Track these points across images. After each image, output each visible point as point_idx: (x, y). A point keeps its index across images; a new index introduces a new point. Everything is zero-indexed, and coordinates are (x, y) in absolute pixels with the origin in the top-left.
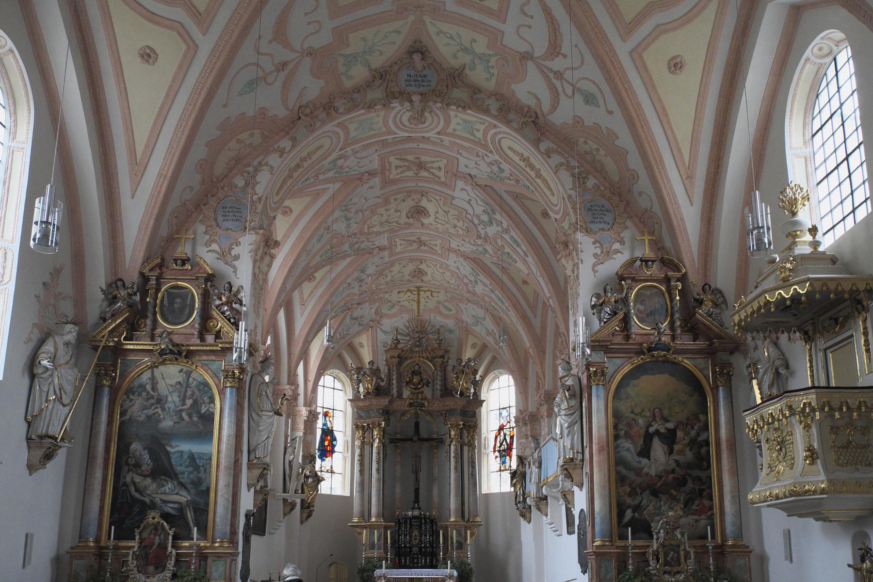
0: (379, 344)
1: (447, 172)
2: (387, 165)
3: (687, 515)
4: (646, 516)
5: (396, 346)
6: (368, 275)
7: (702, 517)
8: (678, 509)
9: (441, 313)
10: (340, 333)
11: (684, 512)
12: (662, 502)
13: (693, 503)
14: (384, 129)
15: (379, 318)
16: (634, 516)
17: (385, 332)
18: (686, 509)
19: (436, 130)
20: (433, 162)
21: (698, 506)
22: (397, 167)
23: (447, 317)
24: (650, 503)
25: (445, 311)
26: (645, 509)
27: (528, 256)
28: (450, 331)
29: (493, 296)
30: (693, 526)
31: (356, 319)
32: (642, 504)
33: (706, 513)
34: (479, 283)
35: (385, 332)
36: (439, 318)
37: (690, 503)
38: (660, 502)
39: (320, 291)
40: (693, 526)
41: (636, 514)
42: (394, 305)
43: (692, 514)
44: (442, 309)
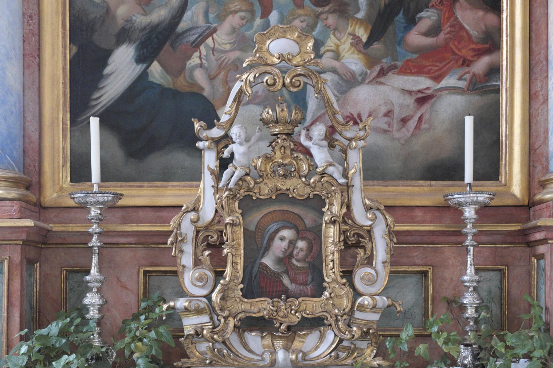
3: (383, 73)
4: (200, 76)
7: (450, 81)
8: (346, 46)
11: (371, 62)
12: (274, 17)
13: (412, 22)
16: (144, 75)
18: (376, 46)
21: (433, 31)
24: (221, 18)
26: (196, 45)
30: (404, 121)
32: (182, 26)
33: (466, 63)
37: (400, 18)
38: (265, 14)
40: (404, 121)
41: (156, 68)
43: (406, 70)
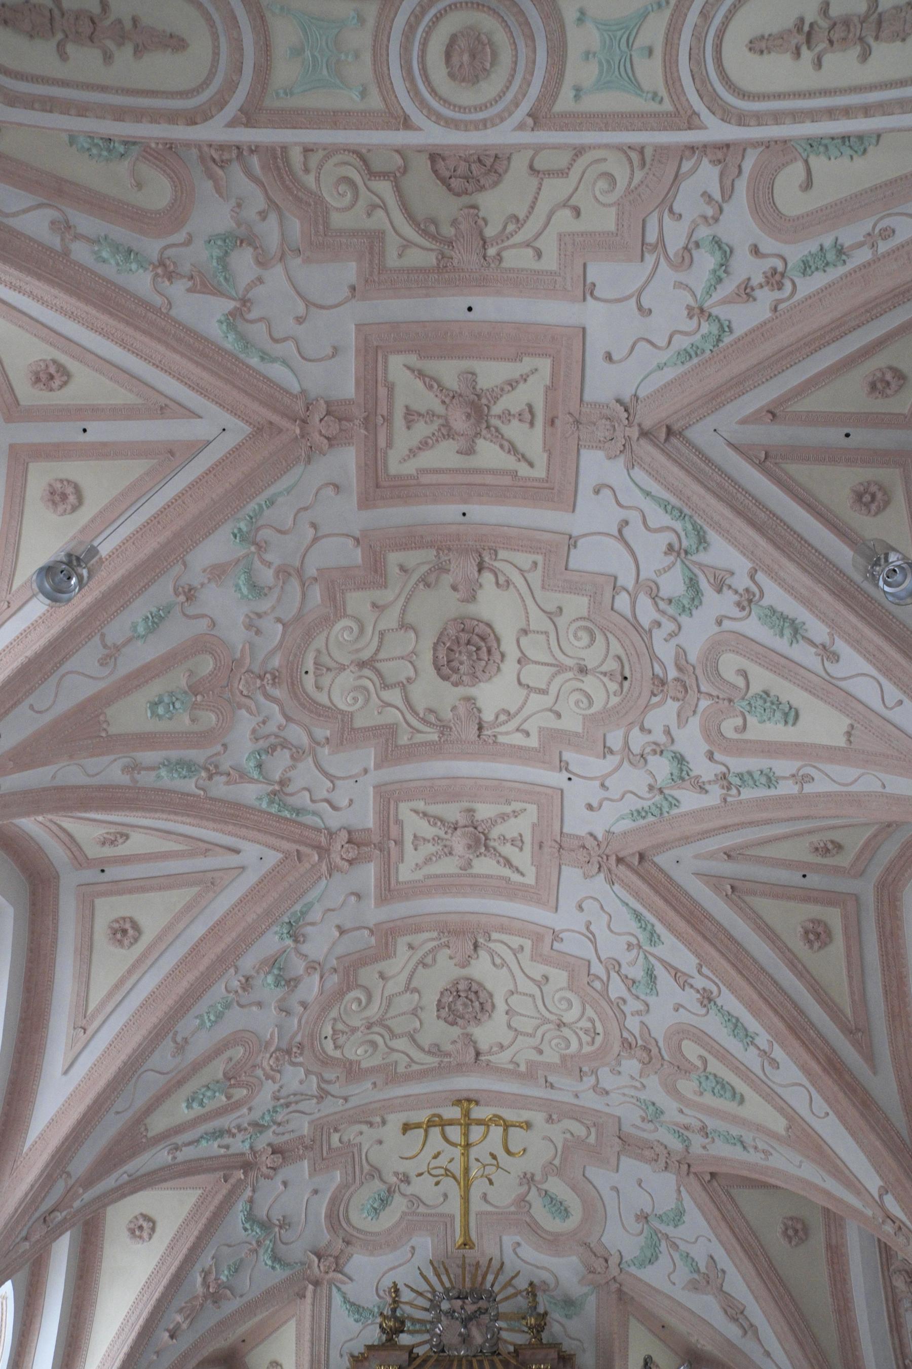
0: (334, 1354)
1: (552, 423)
2: (382, 392)
5: (390, 1340)
6: (313, 966)
9: (534, 1228)
10: (206, 1274)
14: (375, 101)
15: (340, 1244)
17: (356, 1309)
19: (525, 106)
20: (512, 385)
22: (411, 416)
23: (553, 1243)
25: (552, 1224)
27: (835, 657)
28: (570, 1304)
29: (714, 1025)
31: (266, 1226)
34: (663, 977)
35: (356, 1309)
36: (529, 1253)
39: (149, 983)
42: (390, 1191)
44: (540, 1212)
